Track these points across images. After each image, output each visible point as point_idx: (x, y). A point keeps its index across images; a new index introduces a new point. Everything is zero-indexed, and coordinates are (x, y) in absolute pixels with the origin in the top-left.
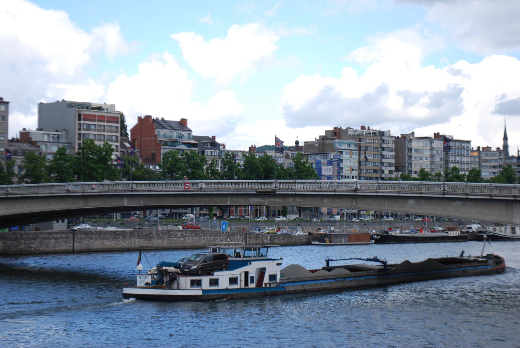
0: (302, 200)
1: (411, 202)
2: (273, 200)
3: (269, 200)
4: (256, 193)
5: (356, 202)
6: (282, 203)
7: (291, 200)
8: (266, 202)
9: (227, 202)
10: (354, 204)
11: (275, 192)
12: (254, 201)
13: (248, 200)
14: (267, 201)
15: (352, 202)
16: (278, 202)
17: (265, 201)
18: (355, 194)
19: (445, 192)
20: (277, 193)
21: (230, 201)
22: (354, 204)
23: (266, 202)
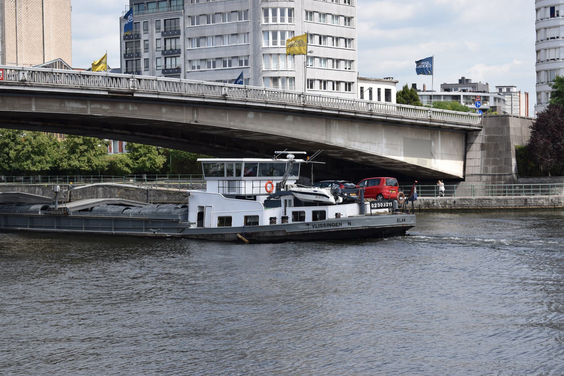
0: (136, 108)
1: (251, 115)
2: (98, 106)
3: (93, 106)
4: (106, 93)
5: (197, 113)
6: (110, 111)
7: (122, 108)
8: (89, 110)
9: (31, 108)
10: (195, 116)
11: (133, 94)
12: (72, 107)
13: (63, 105)
14: (91, 108)
15: (193, 114)
16: (105, 111)
17: (87, 108)
18: (224, 102)
19: (306, 104)
20: (135, 95)
21: (36, 105)
22: (195, 116)
23: (89, 110)
